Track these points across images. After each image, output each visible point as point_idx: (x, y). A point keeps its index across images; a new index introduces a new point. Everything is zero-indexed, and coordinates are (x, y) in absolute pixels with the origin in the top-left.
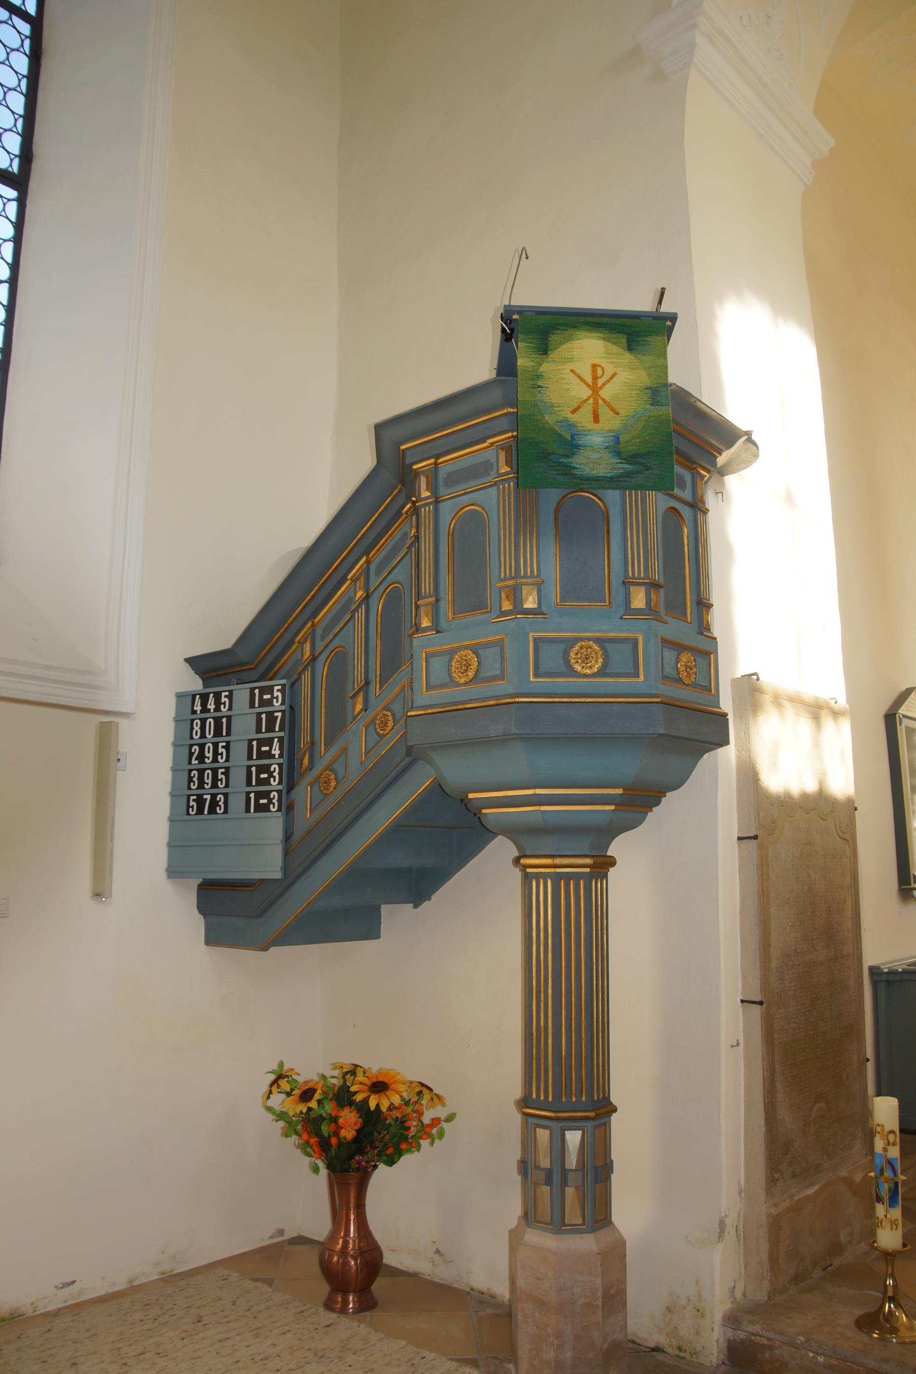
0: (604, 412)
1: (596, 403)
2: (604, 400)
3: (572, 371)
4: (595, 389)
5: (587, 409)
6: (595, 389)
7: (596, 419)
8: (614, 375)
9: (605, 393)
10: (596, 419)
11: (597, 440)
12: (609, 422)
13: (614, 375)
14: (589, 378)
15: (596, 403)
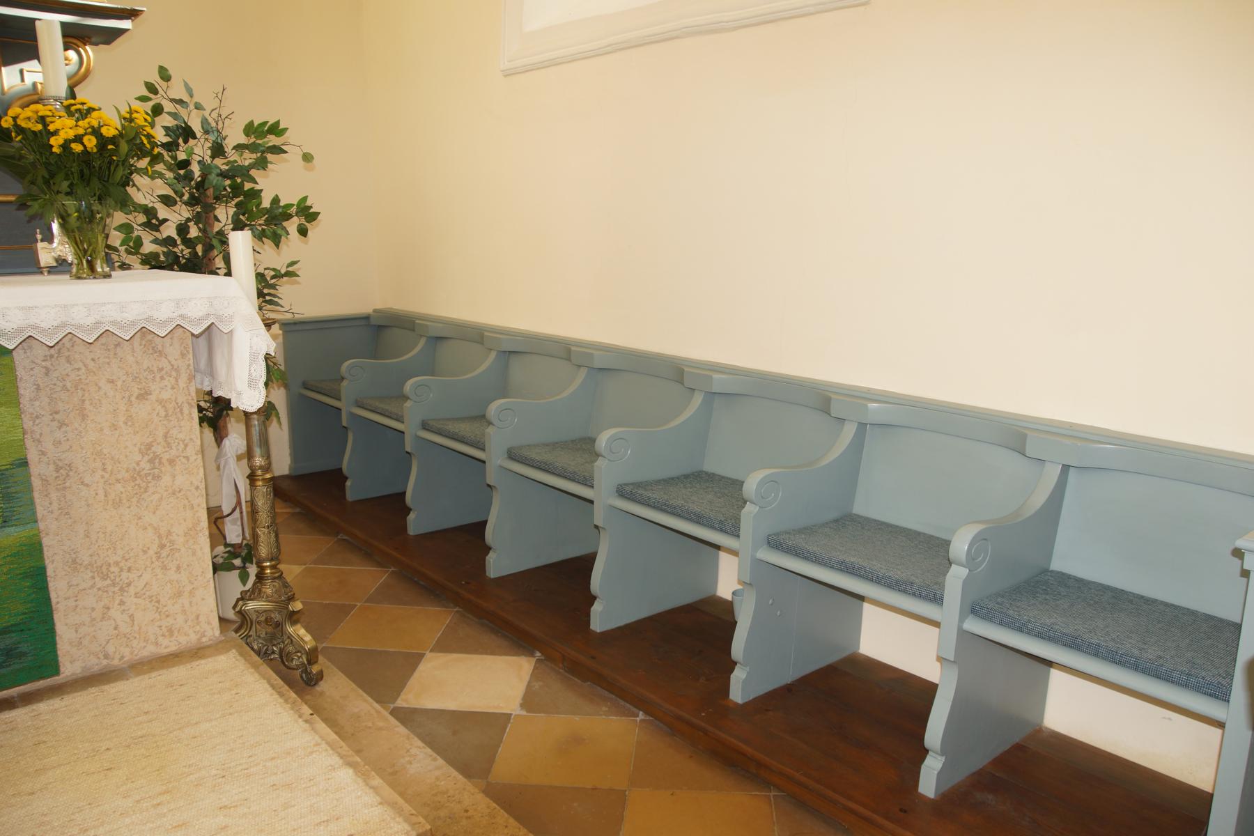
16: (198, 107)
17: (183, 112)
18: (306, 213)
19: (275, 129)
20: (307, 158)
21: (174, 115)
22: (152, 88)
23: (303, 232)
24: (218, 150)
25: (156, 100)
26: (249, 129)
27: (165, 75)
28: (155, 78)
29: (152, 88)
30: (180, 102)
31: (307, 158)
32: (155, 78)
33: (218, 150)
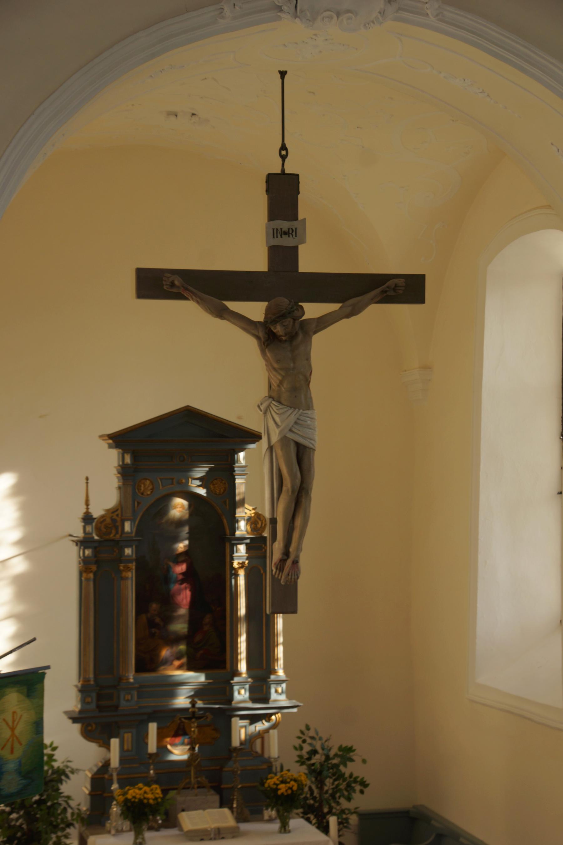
0: (16, 745)
1: (13, 740)
2: (17, 738)
3: (4, 720)
4: (13, 729)
5: (8, 746)
6: (13, 729)
7: (12, 752)
8: (21, 716)
9: (17, 732)
10: (12, 752)
11: (11, 766)
12: (19, 751)
13: (21, 716)
14: (10, 723)
15: (13, 740)
16: (320, 739)
17: (314, 742)
18: (364, 784)
19: (350, 749)
20: (364, 761)
21: (310, 744)
22: (302, 732)
23: (362, 792)
24: (328, 758)
25: (304, 737)
26: (341, 748)
27: (308, 728)
28: (303, 728)
29: (302, 732)
30: (312, 738)
31: (364, 761)
32: (303, 728)
33: (328, 758)
